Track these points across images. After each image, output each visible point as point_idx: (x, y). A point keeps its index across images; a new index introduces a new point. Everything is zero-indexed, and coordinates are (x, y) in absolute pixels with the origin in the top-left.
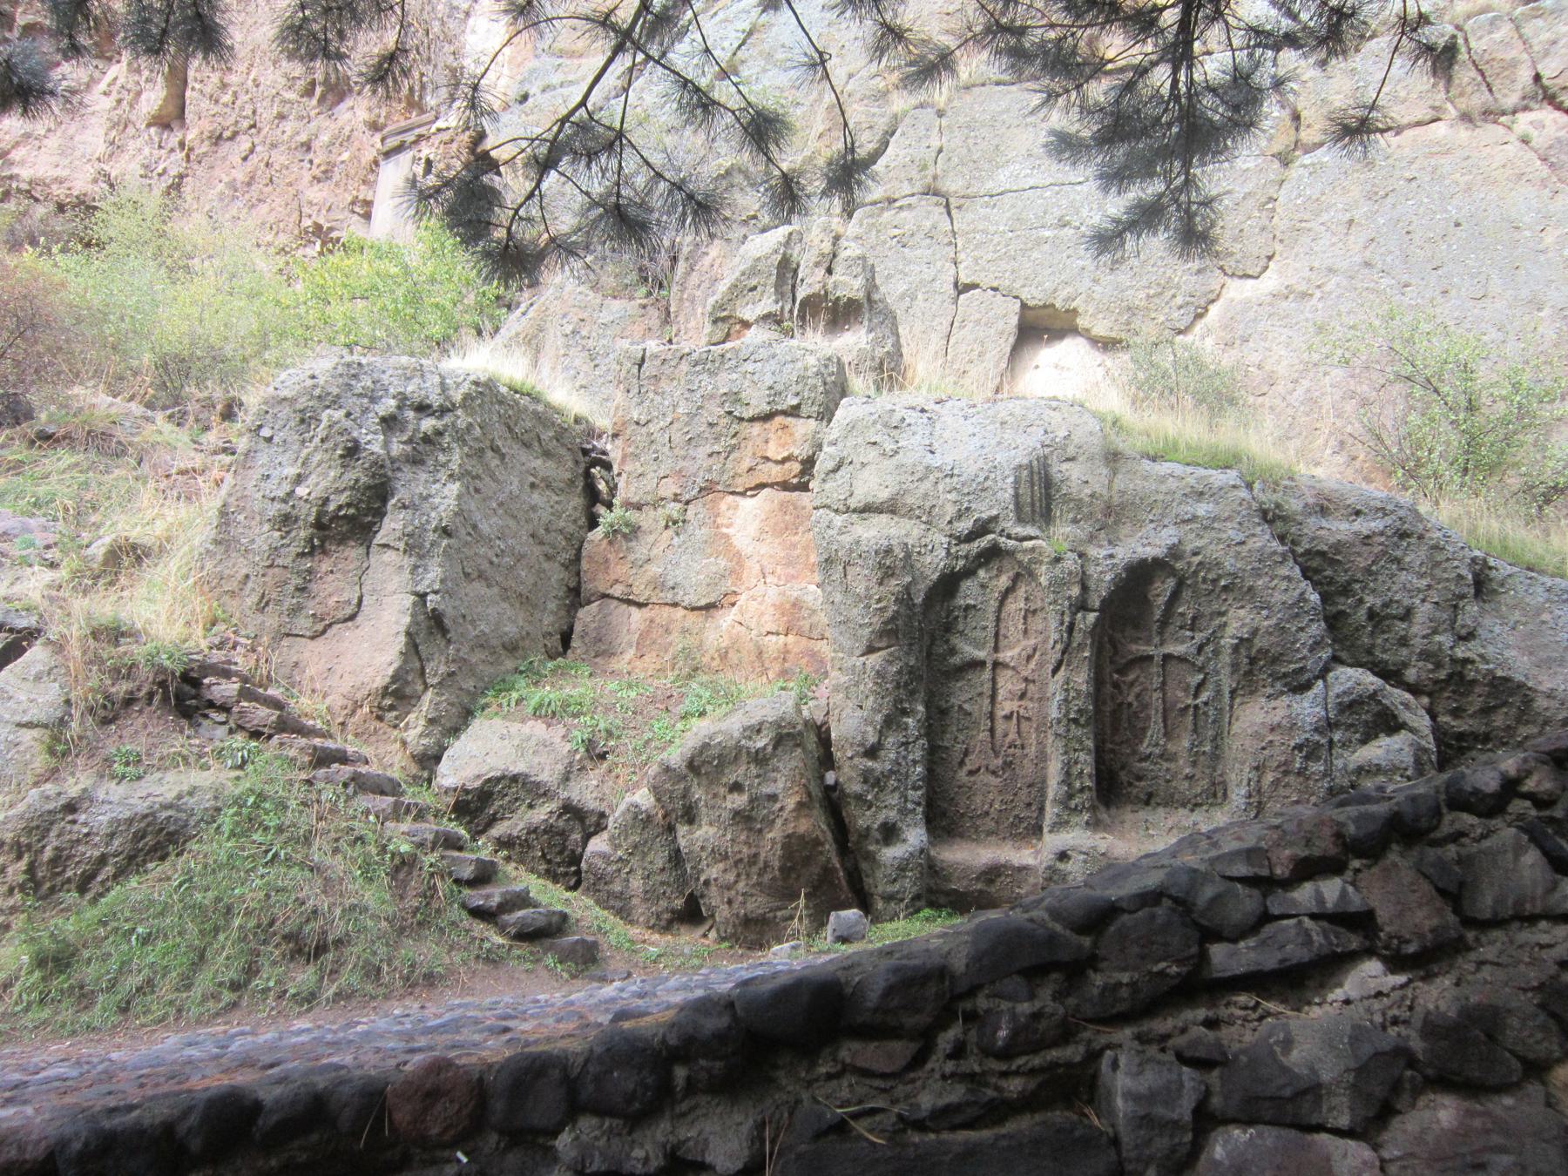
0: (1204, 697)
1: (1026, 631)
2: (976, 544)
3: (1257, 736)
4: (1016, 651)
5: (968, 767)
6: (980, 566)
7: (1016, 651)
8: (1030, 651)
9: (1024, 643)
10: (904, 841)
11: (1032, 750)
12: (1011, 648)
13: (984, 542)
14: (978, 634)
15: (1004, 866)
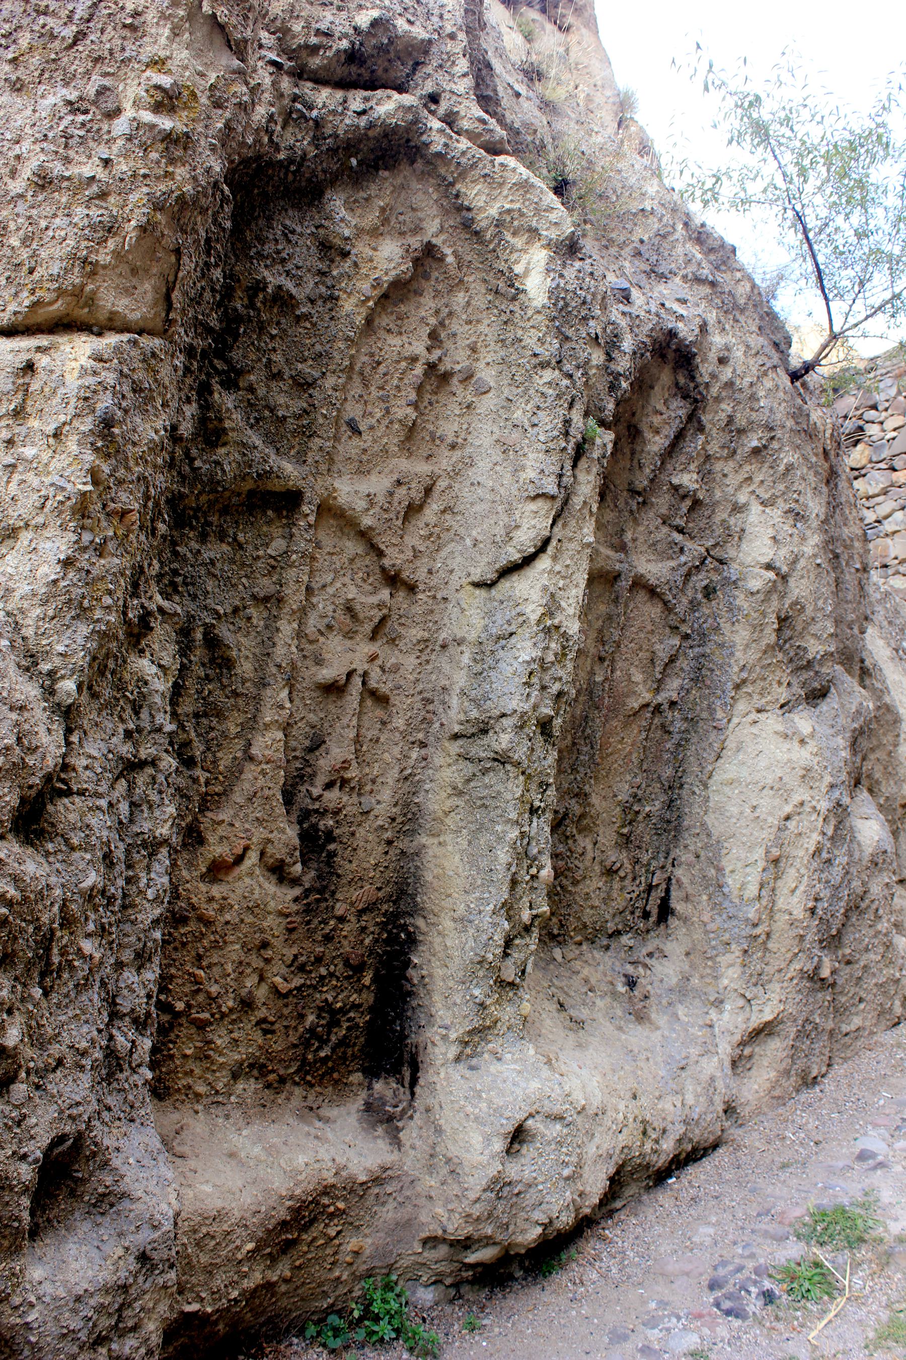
0: (673, 688)
1: (411, 431)
2: (356, 100)
3: (779, 789)
4: (378, 484)
5: (216, 849)
6: (334, 180)
7: (378, 484)
8: (416, 495)
9: (403, 464)
10: (108, 1201)
11: (383, 801)
12: (362, 470)
13: (388, 106)
14: (286, 402)
15: (327, 1190)
